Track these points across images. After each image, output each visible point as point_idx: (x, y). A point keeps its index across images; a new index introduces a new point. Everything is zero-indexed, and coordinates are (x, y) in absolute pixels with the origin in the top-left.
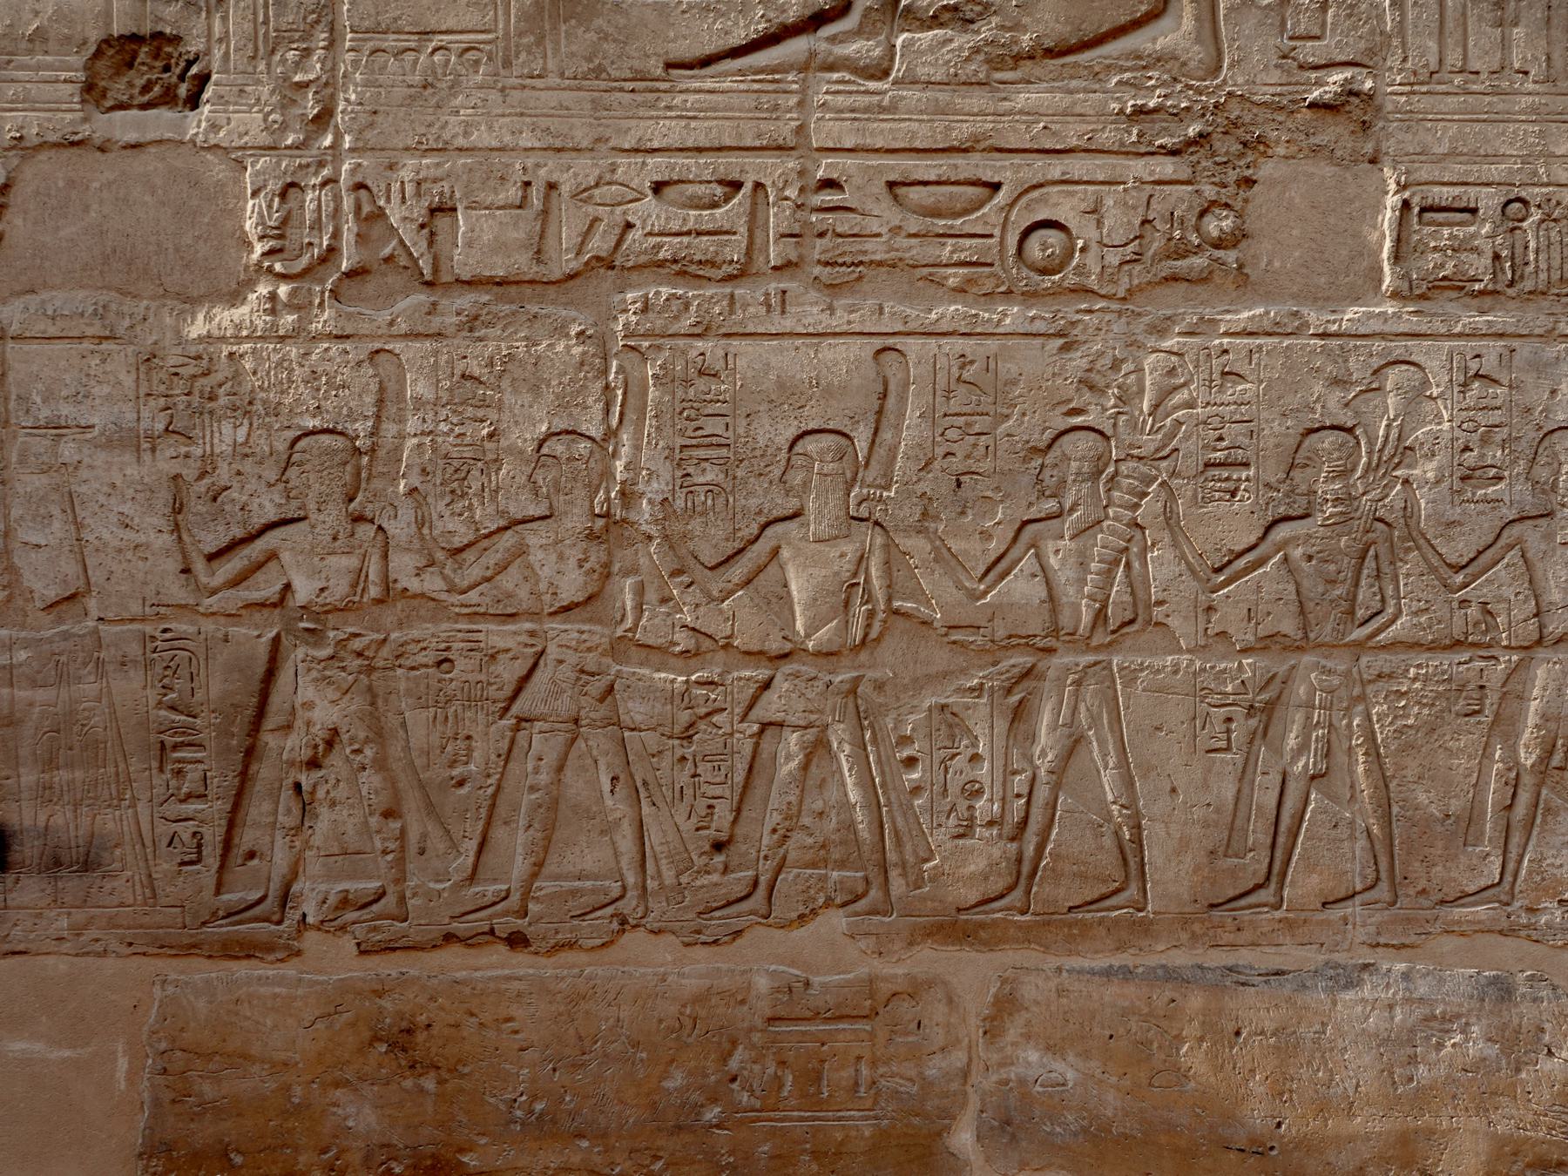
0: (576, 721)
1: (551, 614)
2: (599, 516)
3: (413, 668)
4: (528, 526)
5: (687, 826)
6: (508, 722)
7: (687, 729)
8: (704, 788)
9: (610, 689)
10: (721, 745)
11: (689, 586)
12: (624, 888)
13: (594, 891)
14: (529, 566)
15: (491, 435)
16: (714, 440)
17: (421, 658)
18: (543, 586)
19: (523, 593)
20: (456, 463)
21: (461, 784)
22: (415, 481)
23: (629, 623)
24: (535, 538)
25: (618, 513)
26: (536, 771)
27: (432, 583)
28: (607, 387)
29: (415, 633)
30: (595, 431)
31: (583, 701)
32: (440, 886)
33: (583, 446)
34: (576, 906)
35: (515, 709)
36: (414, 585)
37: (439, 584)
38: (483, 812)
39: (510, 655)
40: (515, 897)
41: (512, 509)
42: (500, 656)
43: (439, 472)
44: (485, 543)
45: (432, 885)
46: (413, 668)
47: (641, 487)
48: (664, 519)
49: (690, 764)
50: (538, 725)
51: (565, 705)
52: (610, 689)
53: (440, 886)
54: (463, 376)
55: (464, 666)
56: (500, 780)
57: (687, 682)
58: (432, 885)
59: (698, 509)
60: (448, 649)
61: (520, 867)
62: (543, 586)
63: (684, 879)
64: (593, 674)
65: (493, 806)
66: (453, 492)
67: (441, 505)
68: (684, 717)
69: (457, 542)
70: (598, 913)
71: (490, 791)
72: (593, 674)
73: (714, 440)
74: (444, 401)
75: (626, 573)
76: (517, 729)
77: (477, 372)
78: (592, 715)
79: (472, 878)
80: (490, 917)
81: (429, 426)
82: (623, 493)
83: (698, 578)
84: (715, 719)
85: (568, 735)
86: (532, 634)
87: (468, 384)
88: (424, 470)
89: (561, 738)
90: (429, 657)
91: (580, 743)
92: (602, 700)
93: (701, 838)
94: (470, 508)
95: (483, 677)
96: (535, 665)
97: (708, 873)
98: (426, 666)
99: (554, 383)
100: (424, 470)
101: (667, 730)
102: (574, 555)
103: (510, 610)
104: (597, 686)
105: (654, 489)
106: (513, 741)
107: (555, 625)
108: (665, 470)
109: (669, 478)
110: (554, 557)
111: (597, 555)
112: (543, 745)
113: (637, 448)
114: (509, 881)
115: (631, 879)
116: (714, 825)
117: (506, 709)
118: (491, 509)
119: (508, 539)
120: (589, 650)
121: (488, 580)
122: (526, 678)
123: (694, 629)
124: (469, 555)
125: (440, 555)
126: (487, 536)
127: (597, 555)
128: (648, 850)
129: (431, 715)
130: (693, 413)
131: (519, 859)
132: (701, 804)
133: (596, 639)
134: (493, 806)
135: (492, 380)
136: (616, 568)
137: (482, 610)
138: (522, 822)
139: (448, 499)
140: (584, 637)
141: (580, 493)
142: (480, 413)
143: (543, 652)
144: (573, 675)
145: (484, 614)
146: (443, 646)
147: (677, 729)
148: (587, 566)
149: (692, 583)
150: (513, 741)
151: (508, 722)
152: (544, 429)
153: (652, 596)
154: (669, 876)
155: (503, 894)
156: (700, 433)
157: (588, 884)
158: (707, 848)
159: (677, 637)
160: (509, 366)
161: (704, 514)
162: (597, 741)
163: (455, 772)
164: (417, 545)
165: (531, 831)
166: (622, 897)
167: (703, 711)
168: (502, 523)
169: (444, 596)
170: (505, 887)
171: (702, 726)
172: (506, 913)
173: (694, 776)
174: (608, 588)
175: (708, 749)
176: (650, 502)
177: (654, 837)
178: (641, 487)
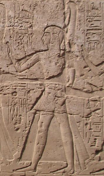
0: (53, 111)
1: (47, 79)
2: (62, 50)
3: (5, 94)
4: (41, 52)
5: (88, 145)
6: (33, 111)
7: (88, 114)
8: (93, 133)
9: (64, 103)
10: (99, 120)
11: (89, 71)
12: (67, 164)
13: (57, 163)
14: (40, 64)
15: (30, 27)
16: (97, 28)
17: (7, 92)
18: (44, 71)
19: (38, 72)
20: (20, 35)
21: (17, 129)
22: (8, 39)
23: (70, 82)
24: (42, 56)
25: (67, 49)
26: (41, 126)
27: (11, 69)
28: (64, 13)
29: (5, 84)
30: (62, 26)
31: (57, 105)
32: (11, 160)
33: (57, 30)
34: (53, 168)
35: (35, 107)
36: (7, 70)
37: (14, 70)
38: (24, 139)
39: (34, 91)
40: (33, 166)
41: (36, 48)
42: (31, 91)
43: (15, 37)
44: (28, 58)
45: (8, 160)
46: (5, 94)
47: (75, 41)
48: (82, 51)
49: (89, 125)
50: (42, 112)
51: (51, 107)
52: (64, 103)
53: (11, 160)
54: (22, 10)
55: (20, 94)
56: (30, 129)
57: (88, 100)
58: (8, 160)
59: (92, 48)
60: (16, 89)
61: (34, 156)
62: (44, 71)
63: (86, 161)
64: (59, 97)
65: (27, 137)
66: (19, 43)
67: (15, 47)
68: (87, 111)
69: (19, 57)
70: (59, 171)
71: (27, 132)
72: (59, 97)
73: (97, 28)
74: (17, 17)
75: (69, 67)
76: (35, 113)
77: (26, 9)
78: (59, 109)
79: (20, 158)
80: (25, 171)
81: (12, 24)
82: (69, 43)
83: (92, 68)
84: (97, 112)
85: (52, 116)
86: (41, 85)
87: (24, 12)
88: (10, 37)
89: (49, 117)
90: (11, 91)
91: (54, 118)
92: (62, 105)
93: (92, 148)
94: (24, 47)
95: (26, 97)
96: (42, 94)
97: (93, 160)
98: (9, 94)
99: (49, 12)
100: (10, 37)
101: (81, 114)
102: (54, 61)
103: (35, 77)
104: (61, 101)
105: (80, 41)
106: (34, 117)
107: (47, 82)
108: (82, 36)
109: (84, 39)
110: (48, 62)
111: (61, 61)
112: (42, 118)
113: (74, 30)
114: (31, 160)
115: (69, 161)
116: (96, 145)
117: (32, 107)
118: (30, 47)
119: (34, 57)
120: (59, 90)
121: (28, 68)
122: (38, 99)
123: (91, 84)
124: (22, 61)
125: (14, 61)
126: (29, 56)
127: (61, 61)
128: (75, 152)
129: (10, 108)
130: (90, 20)
131: (34, 153)
132: (92, 139)
133: (61, 87)
134: (27, 137)
135: (31, 11)
136: (67, 65)
137: (26, 77)
138: (36, 142)
139: (17, 45)
140: (57, 86)
141: (56, 43)
142: (27, 20)
143: (44, 90)
144: (53, 97)
145: (27, 79)
146: (14, 88)
147: (85, 114)
148: (58, 64)
149: (90, 70)
150: (34, 117)
151: (33, 111)
152: (46, 25)
153: (77, 74)
154: (81, 161)
155: (30, 164)
156: (92, 26)
157: (56, 162)
158: (94, 152)
159: (85, 86)
160: (36, 7)
161: (93, 49)
162: (58, 118)
163: (16, 126)
164: (7, 58)
165: (38, 145)
166: (67, 167)
167: (93, 109)
168: (33, 52)
169: (15, 73)
170: (30, 162)
171: (93, 114)
172: (29, 170)
173: (90, 129)
174: (63, 72)
175: (96, 120)
176: (78, 46)
177: (77, 148)
178: (75, 41)
